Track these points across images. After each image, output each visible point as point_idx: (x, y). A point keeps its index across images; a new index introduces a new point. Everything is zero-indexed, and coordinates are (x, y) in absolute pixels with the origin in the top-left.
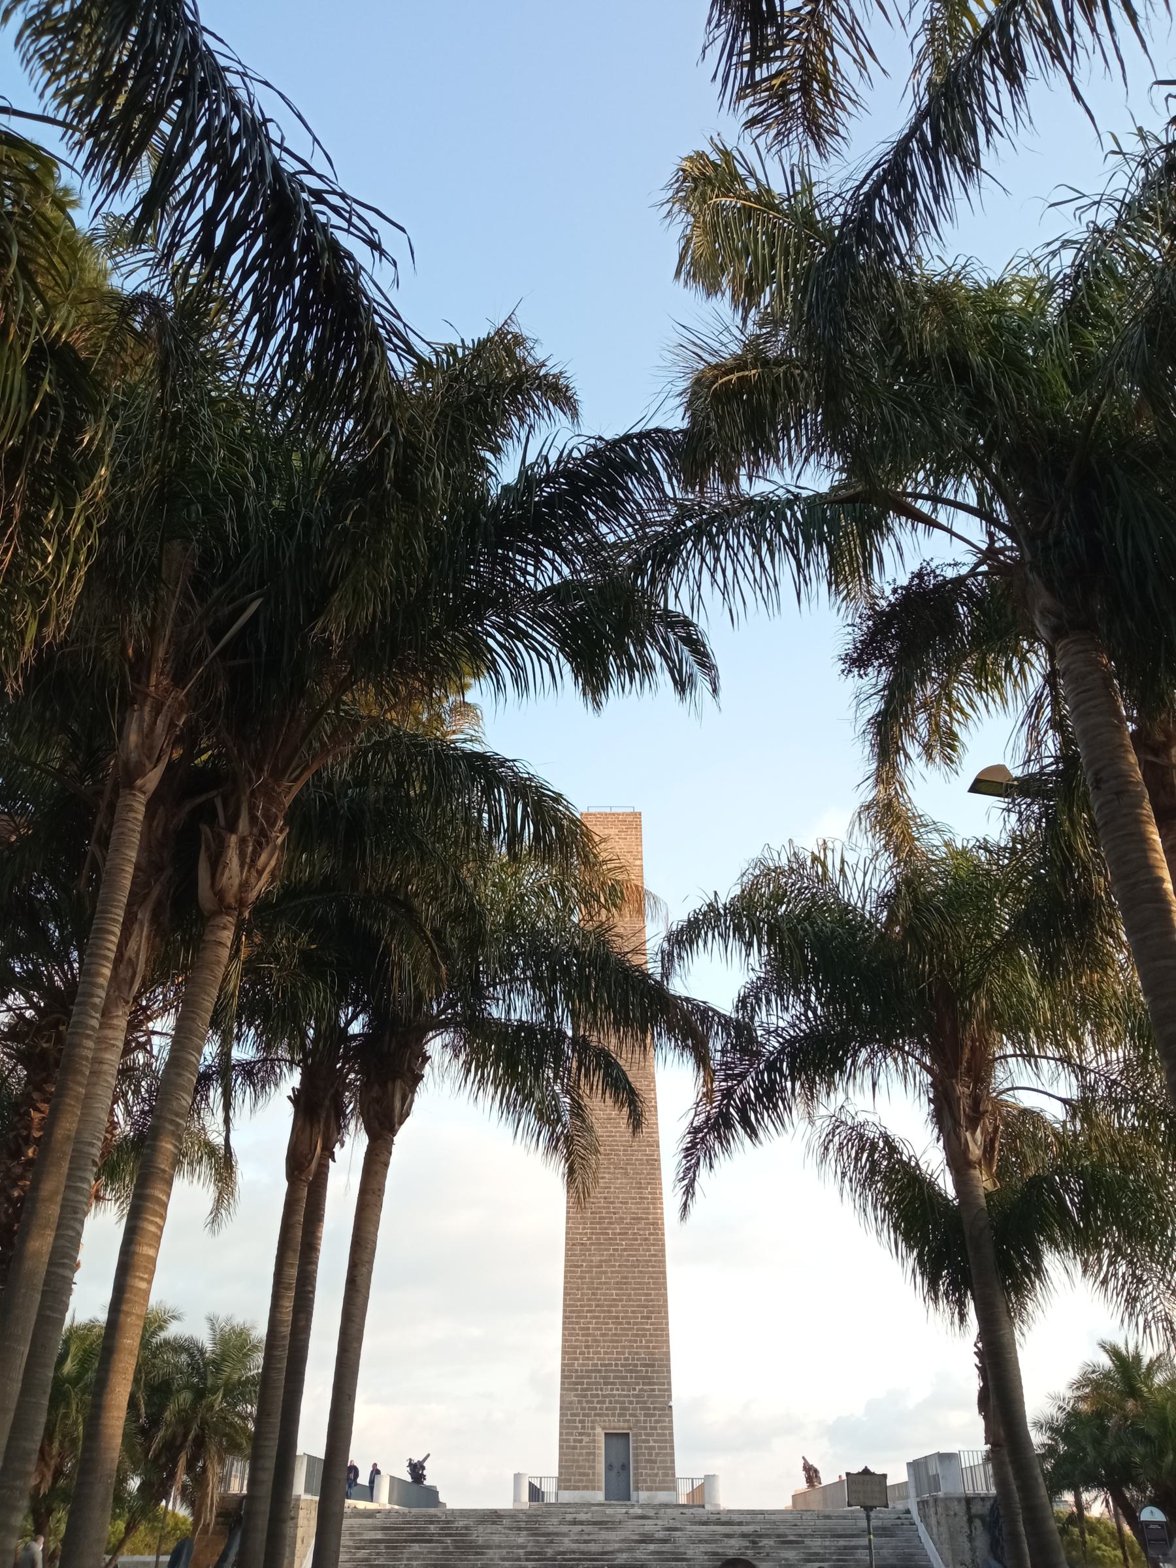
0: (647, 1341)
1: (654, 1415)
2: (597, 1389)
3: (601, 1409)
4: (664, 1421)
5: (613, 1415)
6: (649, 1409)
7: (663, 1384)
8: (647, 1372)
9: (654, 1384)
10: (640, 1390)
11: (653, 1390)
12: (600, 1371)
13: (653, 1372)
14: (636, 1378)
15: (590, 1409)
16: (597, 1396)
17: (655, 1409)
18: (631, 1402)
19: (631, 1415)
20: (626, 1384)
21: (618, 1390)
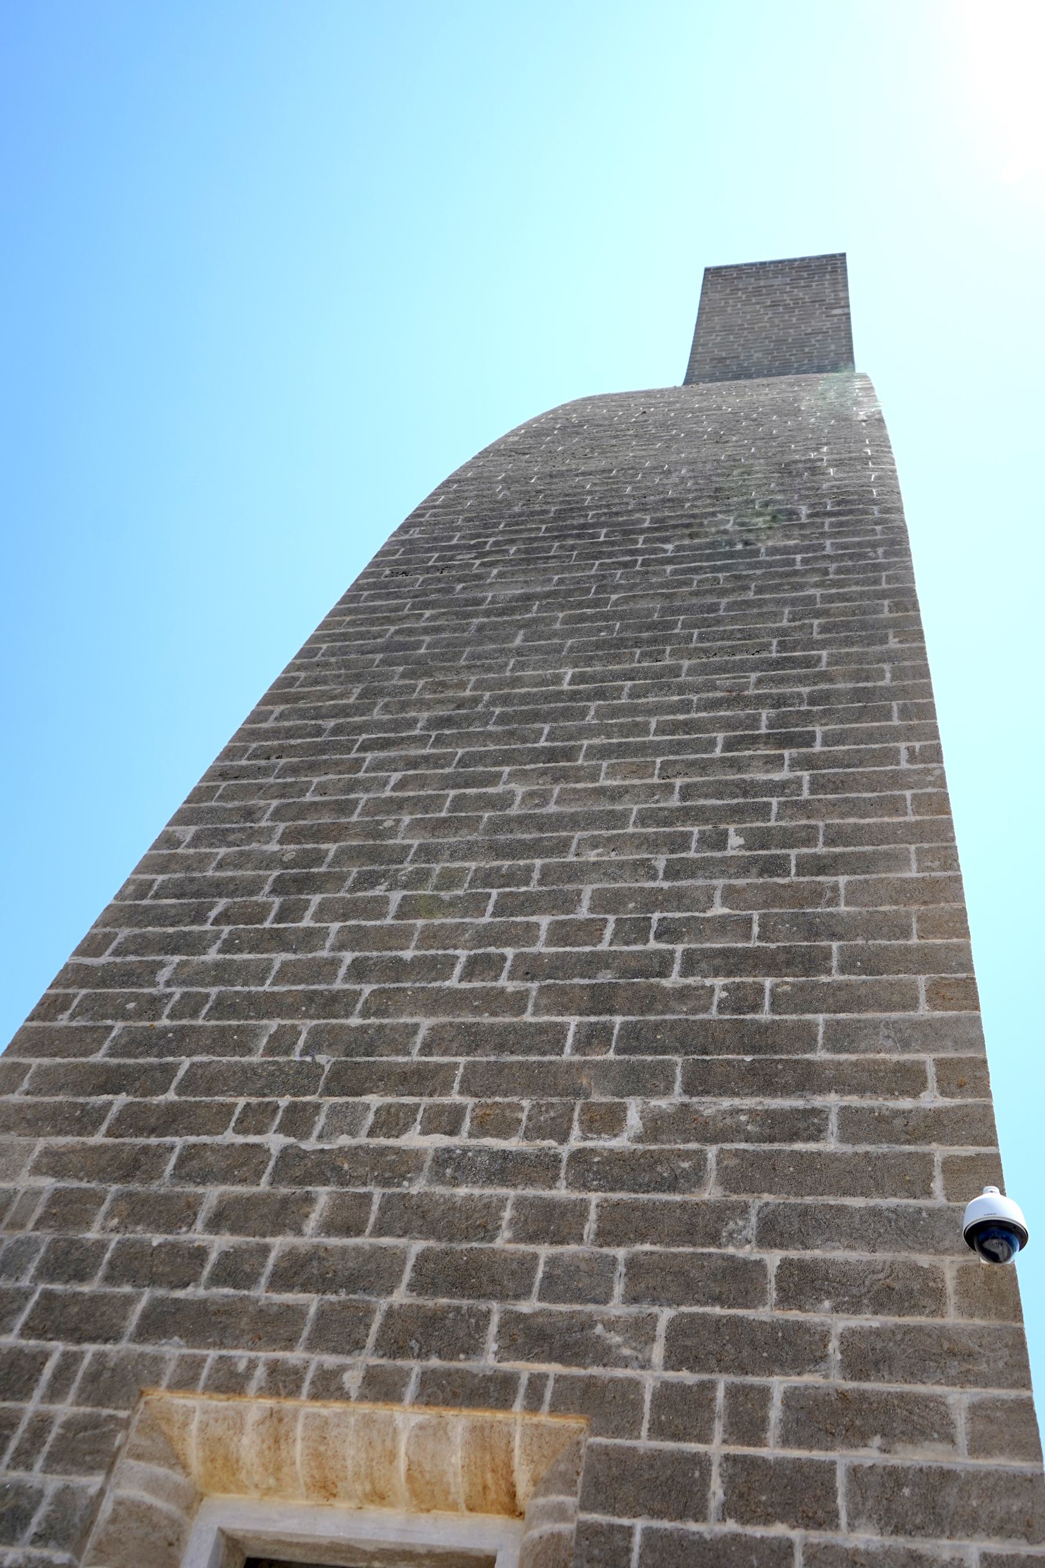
0: (758, 839)
1: (795, 1348)
2: (255, 1119)
3: (233, 1270)
4: (923, 1422)
5: (339, 1331)
6: (741, 1282)
7: (909, 1080)
8: (743, 1000)
9: (809, 1079)
10: (656, 1126)
11: (810, 1124)
12: (334, 1004)
13: (805, 1000)
14: (633, 1040)
15: (131, 1265)
16: (246, 1162)
17: (802, 1283)
18: (548, 1223)
19: (530, 1338)
20: (537, 1080)
21: (448, 1121)
